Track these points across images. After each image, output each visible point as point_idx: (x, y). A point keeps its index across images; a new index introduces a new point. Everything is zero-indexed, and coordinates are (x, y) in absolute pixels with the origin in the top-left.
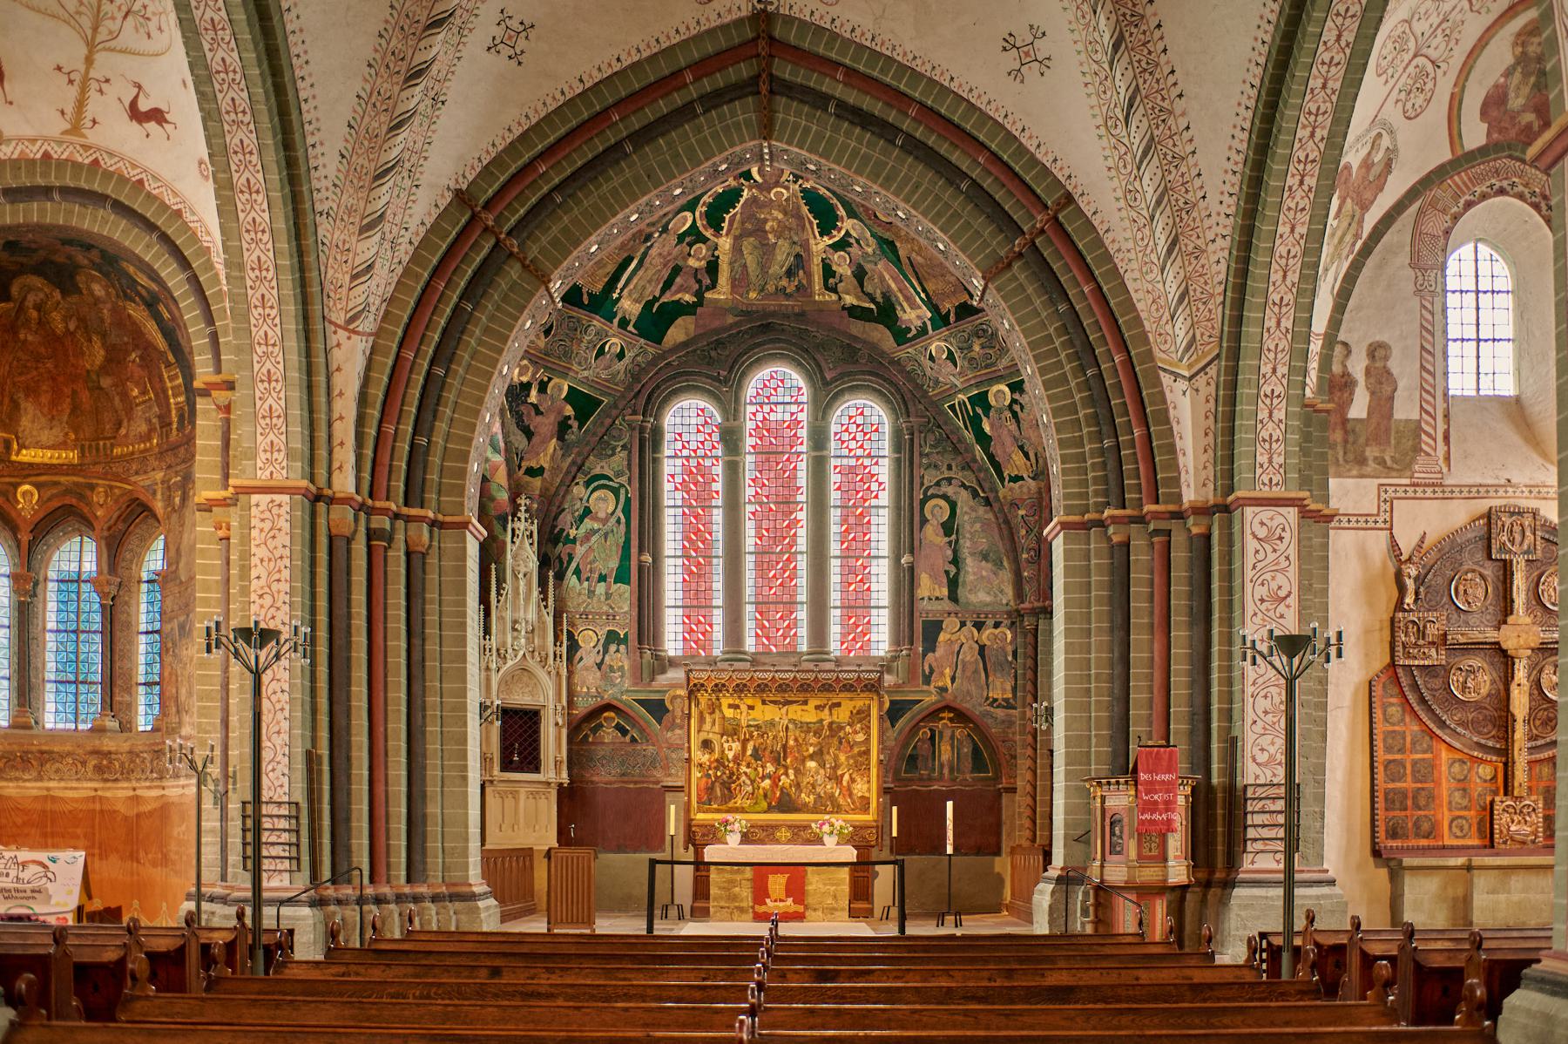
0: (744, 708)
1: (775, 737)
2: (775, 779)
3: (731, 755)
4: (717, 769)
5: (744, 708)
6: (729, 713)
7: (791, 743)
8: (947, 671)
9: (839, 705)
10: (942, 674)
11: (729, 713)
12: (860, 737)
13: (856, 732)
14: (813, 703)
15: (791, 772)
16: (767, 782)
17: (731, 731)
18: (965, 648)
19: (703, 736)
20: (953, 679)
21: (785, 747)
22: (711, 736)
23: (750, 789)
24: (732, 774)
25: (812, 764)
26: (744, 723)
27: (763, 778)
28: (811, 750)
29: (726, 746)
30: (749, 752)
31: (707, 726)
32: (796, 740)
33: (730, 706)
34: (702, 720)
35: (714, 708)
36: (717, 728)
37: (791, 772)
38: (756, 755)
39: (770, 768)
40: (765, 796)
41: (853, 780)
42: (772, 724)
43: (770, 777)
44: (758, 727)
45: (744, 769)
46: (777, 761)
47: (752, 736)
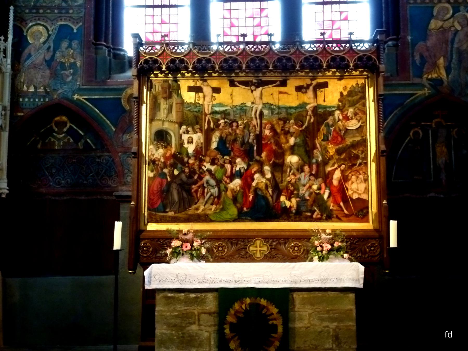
0: (207, 90)
1: (247, 126)
2: (247, 178)
3: (191, 149)
4: (174, 166)
5: (207, 90)
6: (189, 97)
7: (267, 132)
8: (441, 61)
9: (325, 85)
10: (435, 65)
11: (189, 97)
12: (353, 125)
13: (347, 118)
14: (293, 83)
15: (267, 168)
16: (237, 182)
17: (192, 118)
18: (461, 35)
19: (158, 125)
20: (448, 70)
21: (259, 137)
22: (166, 126)
23: (215, 191)
24: (193, 172)
25: (293, 159)
26: (208, 109)
27: (232, 177)
28: (292, 141)
29: (185, 137)
30: (214, 145)
31: (162, 114)
32: (273, 129)
33: (191, 89)
34: (155, 107)
35: (172, 91)
36: (174, 116)
37: (267, 168)
38: (223, 148)
39: (240, 165)
40: (235, 200)
41: (345, 178)
42: (243, 109)
43: (239, 175)
44: (225, 114)
45: (207, 166)
46: (248, 155)
47: (217, 125)
